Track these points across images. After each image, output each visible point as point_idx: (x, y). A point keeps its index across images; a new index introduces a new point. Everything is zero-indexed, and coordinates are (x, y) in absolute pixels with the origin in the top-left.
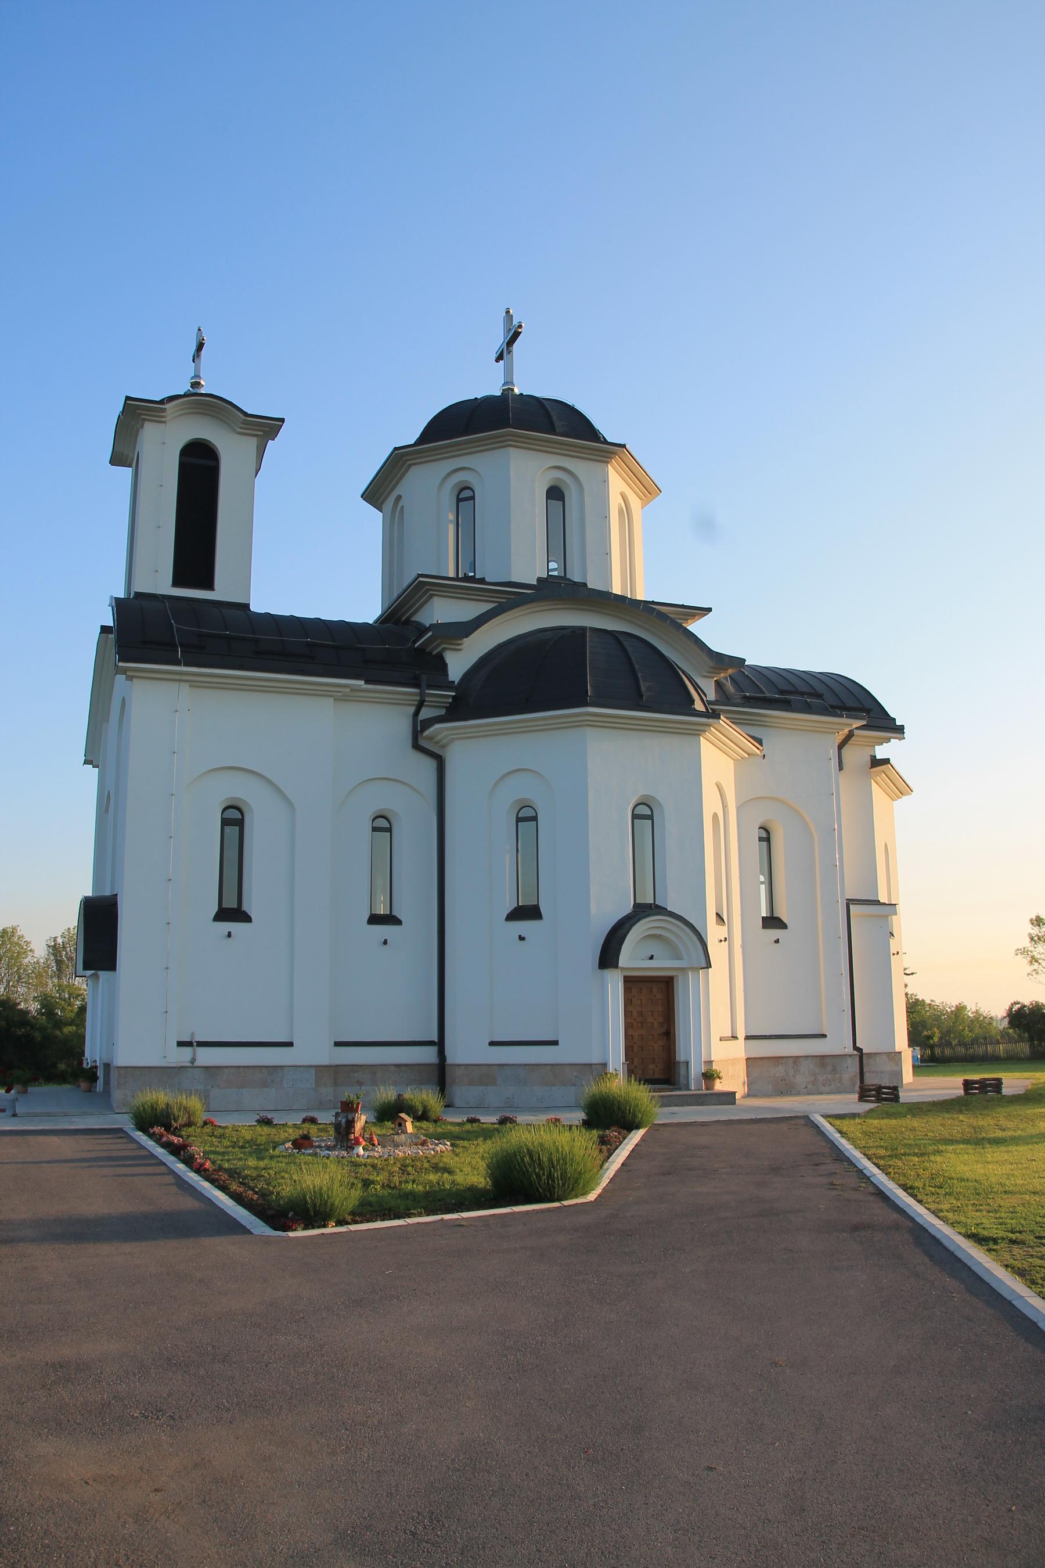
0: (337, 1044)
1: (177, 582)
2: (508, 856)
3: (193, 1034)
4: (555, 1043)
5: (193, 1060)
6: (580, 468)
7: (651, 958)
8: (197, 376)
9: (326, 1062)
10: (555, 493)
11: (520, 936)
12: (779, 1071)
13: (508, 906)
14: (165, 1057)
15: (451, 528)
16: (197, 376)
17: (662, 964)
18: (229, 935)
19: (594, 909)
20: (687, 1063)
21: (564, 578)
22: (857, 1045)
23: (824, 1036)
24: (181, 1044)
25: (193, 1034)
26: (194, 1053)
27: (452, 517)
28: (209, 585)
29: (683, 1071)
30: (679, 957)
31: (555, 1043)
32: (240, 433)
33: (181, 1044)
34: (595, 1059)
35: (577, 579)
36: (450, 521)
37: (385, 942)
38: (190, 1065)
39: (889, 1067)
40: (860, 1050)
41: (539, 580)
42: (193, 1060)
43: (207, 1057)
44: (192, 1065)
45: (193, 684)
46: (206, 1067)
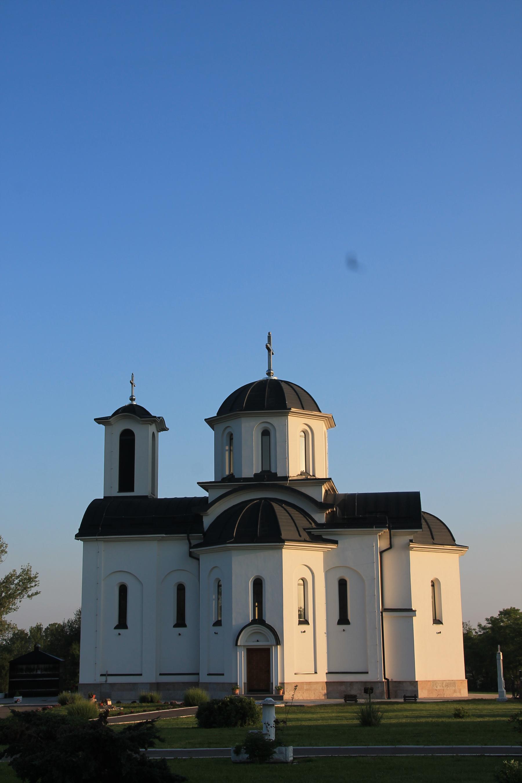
0: (161, 674)
1: (121, 490)
2: (214, 601)
3: (107, 671)
4: (223, 675)
5: (106, 681)
6: (275, 421)
7: (258, 641)
8: (132, 396)
9: (154, 681)
10: (266, 433)
11: (215, 633)
12: (343, 688)
13: (214, 620)
14: (95, 680)
15: (227, 453)
16: (132, 396)
17: (262, 644)
18: (119, 634)
19: (234, 623)
20: (273, 683)
21: (269, 471)
22: (386, 677)
23: (367, 673)
24: (102, 675)
25: (107, 671)
26: (106, 678)
27: (227, 448)
28: (132, 490)
29: (271, 687)
30: (268, 641)
31: (223, 675)
32: (142, 424)
33: (102, 675)
34: (233, 681)
35: (273, 471)
36: (227, 450)
37: (180, 634)
38: (105, 683)
39: (410, 688)
40: (388, 680)
41: (256, 475)
42: (106, 681)
43: (111, 680)
44: (106, 683)
45: (105, 541)
46: (110, 684)
